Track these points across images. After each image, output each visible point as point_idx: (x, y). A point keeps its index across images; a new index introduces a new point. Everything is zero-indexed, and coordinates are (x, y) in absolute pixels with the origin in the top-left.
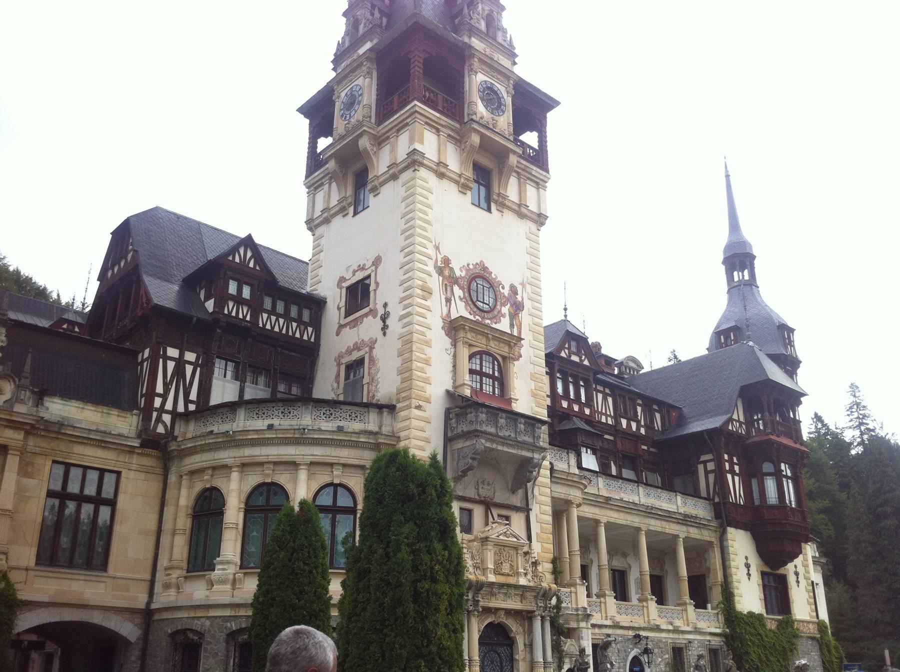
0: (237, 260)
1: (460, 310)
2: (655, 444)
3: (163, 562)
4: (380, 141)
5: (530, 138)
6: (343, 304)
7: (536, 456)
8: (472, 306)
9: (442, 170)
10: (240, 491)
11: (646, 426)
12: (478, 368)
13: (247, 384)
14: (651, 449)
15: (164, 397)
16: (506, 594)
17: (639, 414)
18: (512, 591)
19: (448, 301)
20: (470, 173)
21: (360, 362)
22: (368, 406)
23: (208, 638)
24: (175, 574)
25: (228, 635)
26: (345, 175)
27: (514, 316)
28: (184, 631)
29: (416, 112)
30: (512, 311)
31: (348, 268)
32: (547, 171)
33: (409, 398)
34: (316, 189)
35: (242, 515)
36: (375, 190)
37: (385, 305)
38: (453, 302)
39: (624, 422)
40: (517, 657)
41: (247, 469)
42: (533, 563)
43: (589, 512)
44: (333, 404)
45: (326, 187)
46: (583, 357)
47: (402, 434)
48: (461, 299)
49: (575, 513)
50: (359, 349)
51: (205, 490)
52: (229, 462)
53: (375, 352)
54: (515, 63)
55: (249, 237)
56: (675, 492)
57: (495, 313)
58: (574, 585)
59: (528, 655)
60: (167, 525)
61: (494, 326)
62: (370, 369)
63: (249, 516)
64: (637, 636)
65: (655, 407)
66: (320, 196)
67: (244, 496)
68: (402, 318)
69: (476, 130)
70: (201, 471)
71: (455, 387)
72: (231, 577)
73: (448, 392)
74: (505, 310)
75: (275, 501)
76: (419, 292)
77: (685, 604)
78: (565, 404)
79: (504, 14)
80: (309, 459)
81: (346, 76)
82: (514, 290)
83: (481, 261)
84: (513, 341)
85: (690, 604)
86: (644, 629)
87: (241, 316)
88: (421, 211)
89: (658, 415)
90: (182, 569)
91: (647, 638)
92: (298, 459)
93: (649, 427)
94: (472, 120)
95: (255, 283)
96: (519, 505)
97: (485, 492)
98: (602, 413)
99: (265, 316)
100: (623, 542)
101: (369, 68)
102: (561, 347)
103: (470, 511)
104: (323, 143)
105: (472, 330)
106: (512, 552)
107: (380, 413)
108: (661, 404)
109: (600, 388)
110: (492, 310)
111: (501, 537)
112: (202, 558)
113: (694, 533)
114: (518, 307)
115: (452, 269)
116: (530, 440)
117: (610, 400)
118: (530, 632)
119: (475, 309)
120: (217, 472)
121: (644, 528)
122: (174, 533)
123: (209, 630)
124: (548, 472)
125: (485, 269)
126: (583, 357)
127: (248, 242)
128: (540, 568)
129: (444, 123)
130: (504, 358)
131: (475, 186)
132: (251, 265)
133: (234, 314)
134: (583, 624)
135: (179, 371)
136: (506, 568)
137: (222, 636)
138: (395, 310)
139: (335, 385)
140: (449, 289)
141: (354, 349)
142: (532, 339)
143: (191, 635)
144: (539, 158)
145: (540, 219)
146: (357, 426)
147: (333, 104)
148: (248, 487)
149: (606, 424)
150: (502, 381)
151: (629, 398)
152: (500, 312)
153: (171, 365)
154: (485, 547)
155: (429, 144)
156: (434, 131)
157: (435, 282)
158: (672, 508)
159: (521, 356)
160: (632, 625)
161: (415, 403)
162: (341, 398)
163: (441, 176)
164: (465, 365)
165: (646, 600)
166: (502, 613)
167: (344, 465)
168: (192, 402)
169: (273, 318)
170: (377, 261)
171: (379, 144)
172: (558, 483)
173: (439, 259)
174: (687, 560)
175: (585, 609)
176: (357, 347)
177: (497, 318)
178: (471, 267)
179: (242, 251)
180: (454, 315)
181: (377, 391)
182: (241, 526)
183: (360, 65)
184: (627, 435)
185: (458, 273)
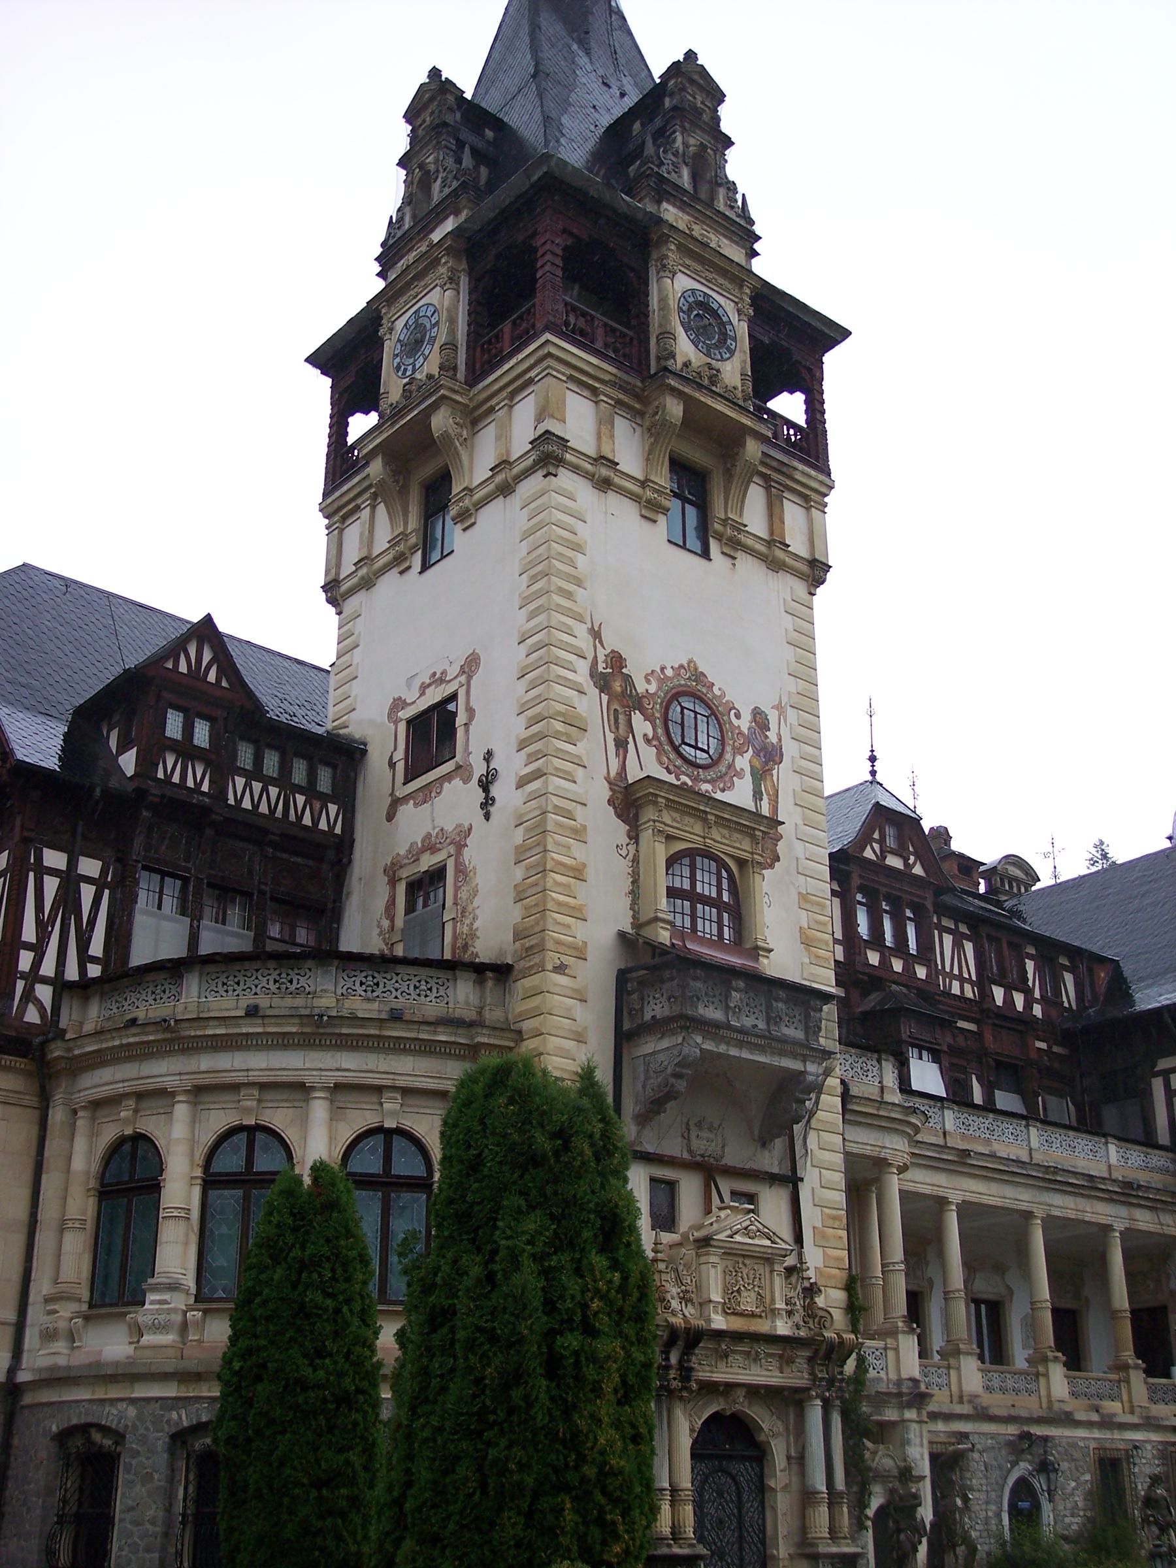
0: (183, 668)
1: (646, 763)
2: (1066, 1038)
3: (41, 1286)
5: (790, 405)
6: (400, 754)
7: (811, 1068)
8: (672, 756)
9: (605, 472)
10: (192, 1142)
11: (1044, 1000)
12: (686, 885)
13: (205, 922)
14: (1055, 1049)
15: (39, 950)
16: (748, 1353)
17: (1030, 976)
18: (762, 1349)
19: (621, 744)
20: (663, 478)
21: (437, 875)
22: (451, 967)
23: (132, 1442)
24: (66, 1310)
25: (174, 1437)
26: (403, 491)
27: (761, 775)
28: (84, 1429)
29: (549, 355)
30: (757, 764)
31: (410, 680)
32: (829, 474)
33: (540, 948)
34: (344, 519)
35: (197, 1191)
36: (466, 518)
37: (489, 756)
38: (631, 746)
39: (998, 993)
40: (772, 1483)
41: (205, 1098)
42: (805, 1289)
43: (924, 1181)
44: (383, 963)
45: (365, 514)
46: (912, 859)
47: (527, 1025)
48: (648, 741)
49: (894, 1184)
51: (121, 1141)
52: (170, 1082)
54: (755, 254)
55: (208, 619)
56: (1105, 1135)
58: (893, 1333)
59: (795, 1479)
60: (48, 1212)
61: (719, 796)
62: (457, 889)
63: (212, 1194)
64: (1026, 1436)
65: (1063, 960)
66: (353, 534)
67: (200, 1153)
68: (522, 783)
69: (673, 390)
70: (114, 1101)
71: (638, 925)
72: (178, 1318)
73: (622, 935)
74: (743, 762)
75: (264, 1162)
76: (559, 726)
77: (1125, 1367)
78: (874, 958)
79: (730, 154)
80: (331, 1078)
81: (407, 286)
82: (760, 720)
83: (690, 661)
84: (762, 828)
85: (1137, 1367)
86: (1040, 1421)
87: (190, 783)
88: (561, 557)
89: (1069, 978)
90: (80, 1300)
91: (1046, 1439)
92: (309, 1079)
93: (1051, 1001)
94: (666, 369)
95: (218, 713)
96: (776, 1170)
97: (703, 1144)
98: (952, 976)
99: (240, 782)
100: (995, 1242)
101: (452, 270)
102: (864, 838)
103: (671, 1185)
104: (360, 424)
105: (671, 805)
106: (761, 1269)
107: (480, 983)
108: (1076, 954)
109: (947, 923)
110: (715, 763)
111: (738, 1238)
112: (119, 1280)
113: (1145, 1220)
114: (770, 756)
115: (628, 679)
116: (800, 1035)
117: (969, 947)
118: (800, 1430)
119: (679, 762)
120: (144, 1104)
121: (1039, 1212)
122: (62, 1227)
123: (135, 1426)
124: (838, 1101)
125: (699, 677)
126: (912, 859)
127: (206, 629)
128: (820, 1301)
129: (607, 378)
130: (742, 863)
131: (675, 505)
132: (212, 677)
133: (176, 779)
134: (911, 1414)
135: (68, 898)
136: (748, 1302)
137: (160, 1440)
138: (510, 765)
139: (386, 923)
140: (622, 718)
141: (423, 850)
142: (800, 822)
143: (97, 1437)
144: (811, 443)
145: (815, 571)
146: (431, 1007)
147: (380, 343)
148: (207, 1137)
149: (961, 998)
150: (737, 911)
151: (1010, 944)
152: (731, 766)
153: (51, 885)
154: (703, 1259)
155: (579, 420)
156: (586, 393)
157: (591, 705)
158: (1099, 1170)
159: (778, 859)
160: (1013, 1412)
161: (552, 958)
162: (399, 951)
163: (604, 485)
165: (1045, 1360)
166: (741, 1393)
167: (406, 1091)
168: (94, 960)
169: (257, 786)
170: (471, 665)
171: (475, 422)
172: (859, 1124)
173: (601, 658)
174: (1129, 1275)
175: (915, 1381)
176: (430, 846)
177: (726, 779)
178: (669, 673)
179: (192, 650)
181: (473, 935)
182: (195, 1214)
183: (435, 262)
184: (1006, 1019)
185: (641, 687)
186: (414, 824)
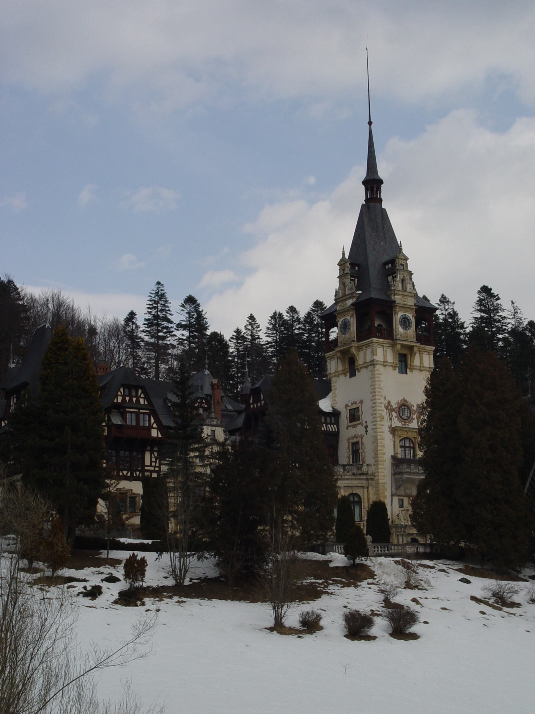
4: (359, 348)
9: (385, 364)
19: (391, 419)
31: (349, 401)
37: (366, 422)
47: (376, 474)
50: (357, 438)
53: (363, 440)
57: (410, 419)
71: (395, 454)
73: (392, 456)
88: (378, 385)
103: (402, 499)
105: (400, 430)
110: (409, 418)
115: (391, 405)
125: (405, 401)
157: (385, 413)
163: (385, 366)
164: (398, 444)
170: (361, 402)
176: (356, 437)
180: (393, 426)
183: (348, 311)
185: (394, 406)
186: (352, 432)
